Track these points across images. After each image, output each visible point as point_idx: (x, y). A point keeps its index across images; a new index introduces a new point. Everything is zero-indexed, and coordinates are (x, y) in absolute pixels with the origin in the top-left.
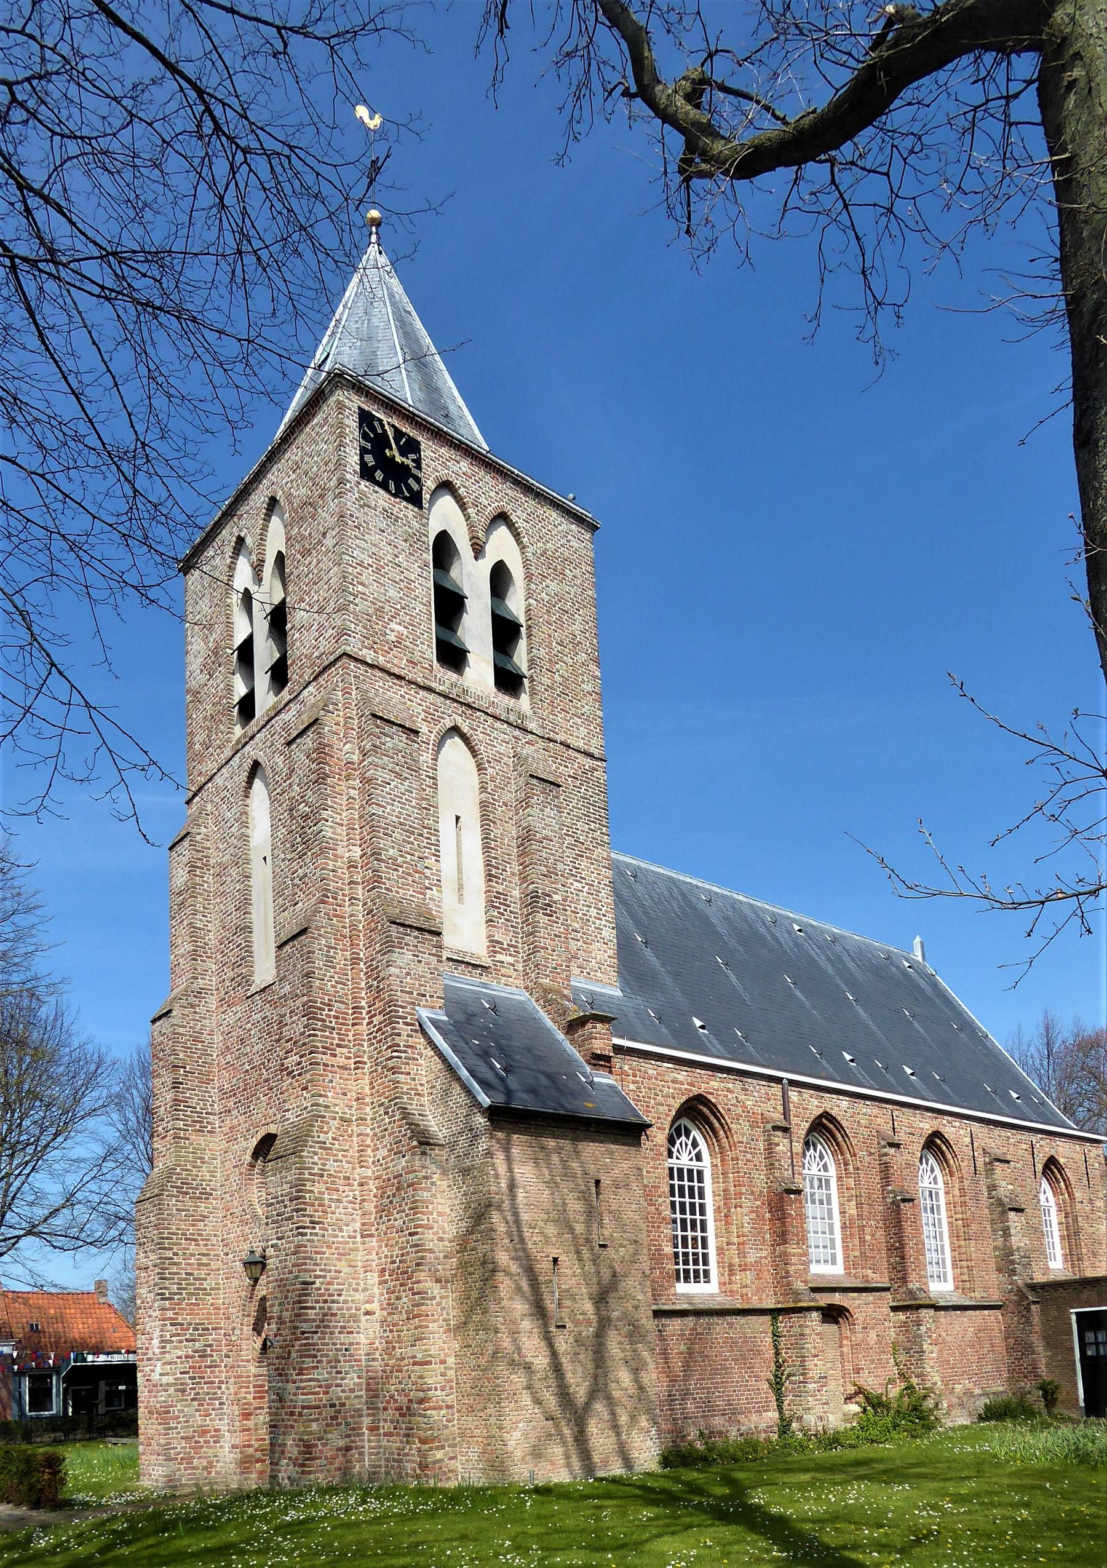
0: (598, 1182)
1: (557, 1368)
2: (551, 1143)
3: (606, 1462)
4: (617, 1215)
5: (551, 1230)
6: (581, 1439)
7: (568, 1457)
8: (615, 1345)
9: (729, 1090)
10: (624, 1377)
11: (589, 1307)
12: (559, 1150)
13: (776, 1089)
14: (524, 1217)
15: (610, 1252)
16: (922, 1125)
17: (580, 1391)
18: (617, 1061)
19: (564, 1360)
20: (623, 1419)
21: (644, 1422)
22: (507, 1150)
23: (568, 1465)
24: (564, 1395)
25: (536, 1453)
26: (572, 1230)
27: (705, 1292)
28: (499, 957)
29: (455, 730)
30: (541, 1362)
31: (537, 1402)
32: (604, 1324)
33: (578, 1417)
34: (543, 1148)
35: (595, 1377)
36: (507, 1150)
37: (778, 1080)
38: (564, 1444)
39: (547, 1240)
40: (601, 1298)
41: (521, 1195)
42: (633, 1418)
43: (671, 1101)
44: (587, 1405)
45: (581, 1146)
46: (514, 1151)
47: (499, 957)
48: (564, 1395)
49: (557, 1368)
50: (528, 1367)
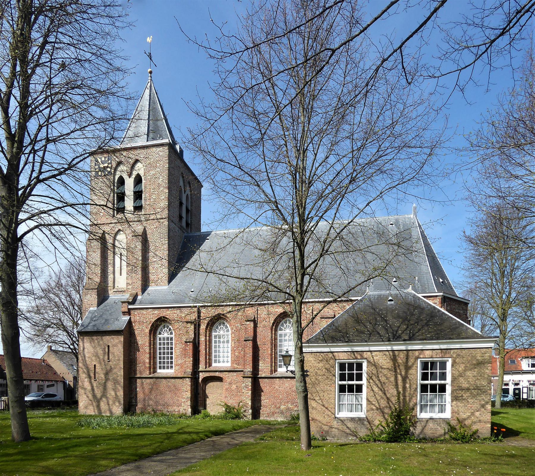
0: (108, 346)
1: (93, 389)
2: (95, 338)
3: (105, 412)
4: (113, 353)
5: (94, 358)
6: (98, 406)
7: (94, 409)
8: (110, 385)
9: (175, 313)
10: (113, 393)
11: (103, 376)
12: (97, 339)
13: (196, 309)
14: (87, 355)
15: (110, 363)
16: (276, 310)
17: (99, 395)
18: (132, 312)
19: (95, 388)
20: (111, 403)
21: (117, 404)
22: (83, 340)
23: (94, 411)
24: (94, 396)
25: (86, 407)
26: (99, 358)
27: (169, 372)
28: (128, 287)
29: (119, 230)
30: (89, 388)
31: (88, 397)
32: (107, 379)
33: (98, 401)
34: (93, 339)
35: (104, 392)
36: (83, 340)
37: (196, 307)
38: (93, 406)
39: (92, 360)
40: (107, 374)
41: (86, 350)
42: (114, 403)
43: (151, 320)
44: (101, 399)
45: (104, 338)
46: (85, 341)
47: (128, 287)
48: (94, 396)
49: (93, 389)
50: (85, 389)
